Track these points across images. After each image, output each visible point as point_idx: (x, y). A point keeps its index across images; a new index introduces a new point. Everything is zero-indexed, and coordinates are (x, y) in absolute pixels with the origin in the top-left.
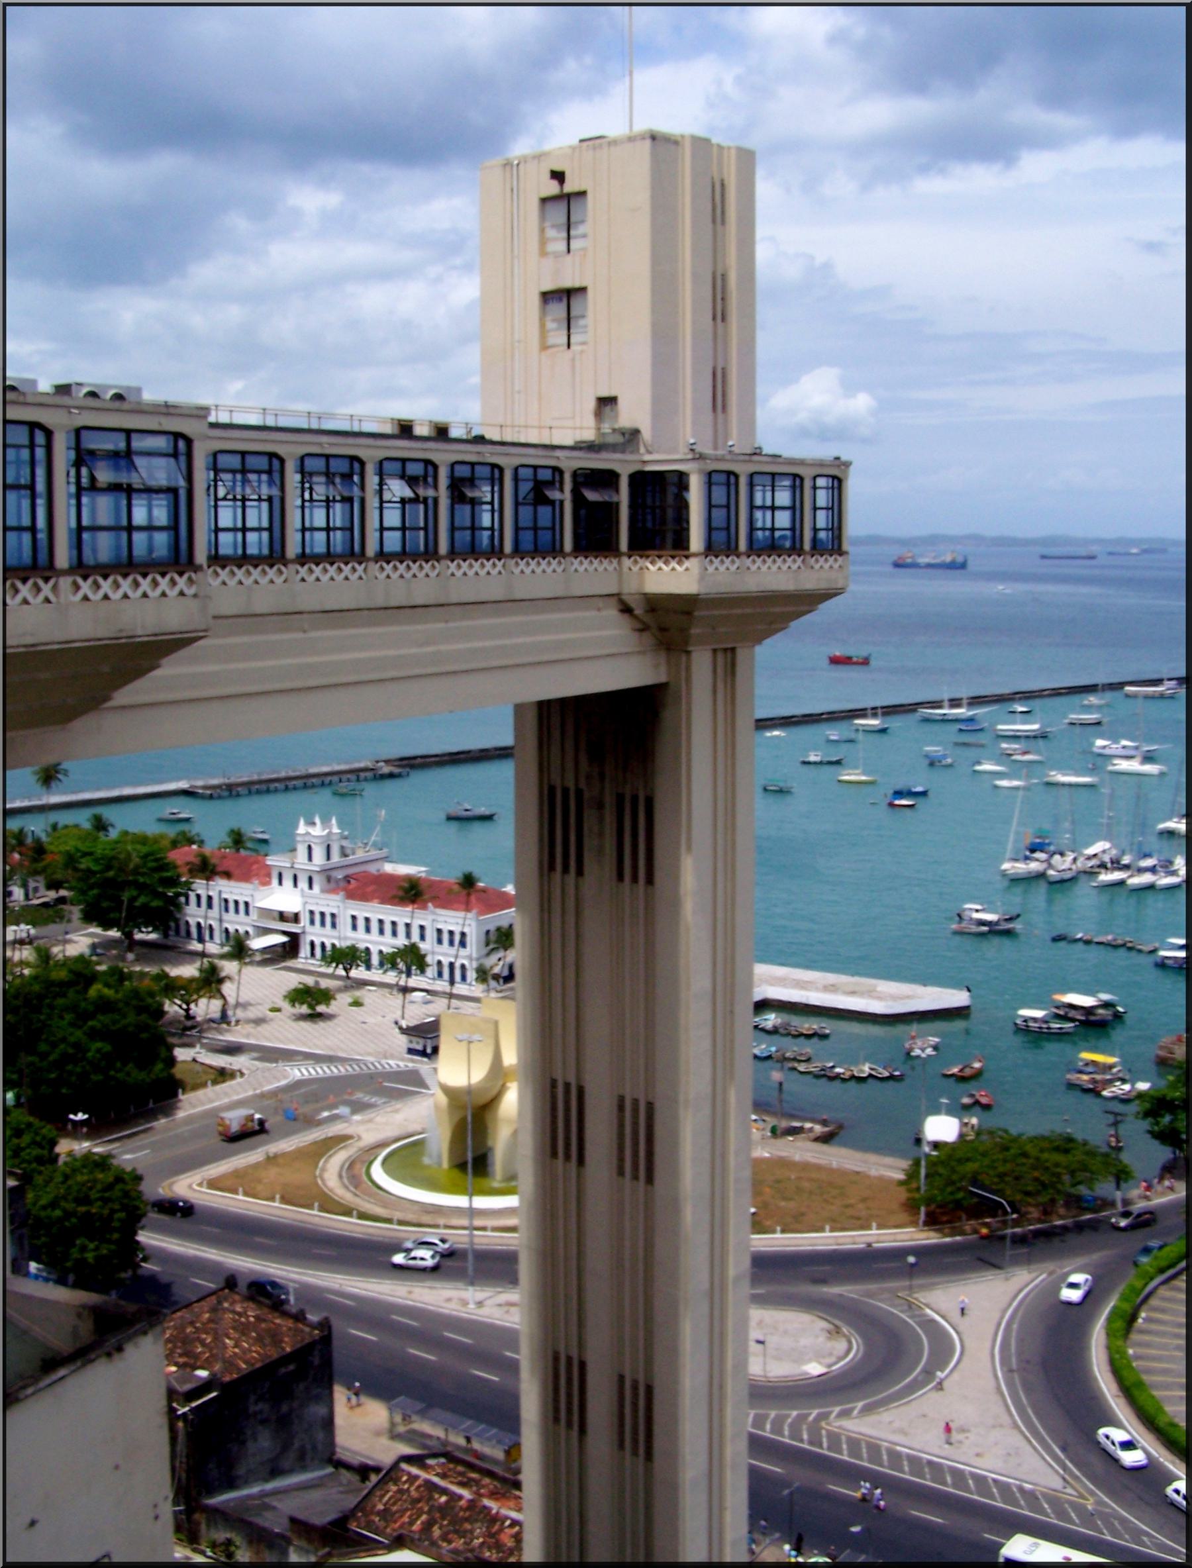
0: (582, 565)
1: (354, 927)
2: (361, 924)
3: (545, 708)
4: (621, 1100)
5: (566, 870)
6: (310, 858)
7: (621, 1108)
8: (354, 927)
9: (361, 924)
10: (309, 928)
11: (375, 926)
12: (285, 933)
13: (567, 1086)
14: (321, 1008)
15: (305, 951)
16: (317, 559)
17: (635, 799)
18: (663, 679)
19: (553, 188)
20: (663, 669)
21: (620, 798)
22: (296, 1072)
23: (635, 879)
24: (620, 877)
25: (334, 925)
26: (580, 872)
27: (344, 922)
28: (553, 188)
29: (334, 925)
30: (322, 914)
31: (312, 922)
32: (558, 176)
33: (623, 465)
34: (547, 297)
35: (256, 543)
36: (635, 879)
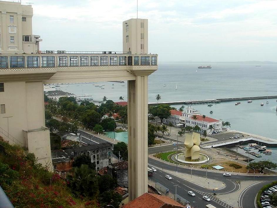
1: (192, 123)
6: (188, 112)
8: (192, 123)
12: (183, 124)
15: (185, 126)
18: (135, 79)
20: (135, 78)
22: (174, 143)
28: (126, 25)
30: (188, 121)
34: (127, 36)
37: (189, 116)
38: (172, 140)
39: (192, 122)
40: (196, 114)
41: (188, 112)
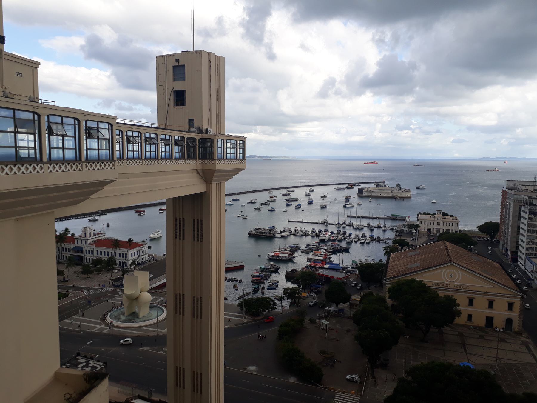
0: (187, 161)
1: (98, 254)
2: (99, 253)
3: (174, 199)
4: (194, 297)
5: (180, 239)
6: (85, 236)
7: (194, 300)
8: (98, 254)
9: (99, 253)
10: (85, 254)
11: (103, 253)
13: (180, 294)
14: (90, 275)
15: (84, 260)
16: (131, 159)
17: (198, 221)
19: (177, 64)
21: (194, 220)
23: (198, 241)
24: (194, 240)
25: (92, 254)
26: (183, 239)
27: (95, 253)
29: (92, 254)
31: (86, 253)
33: (197, 136)
35: (104, 153)
36: (198, 241)
37: (88, 242)
38: (80, 289)
39: (97, 251)
40: (103, 237)
41: (85, 236)
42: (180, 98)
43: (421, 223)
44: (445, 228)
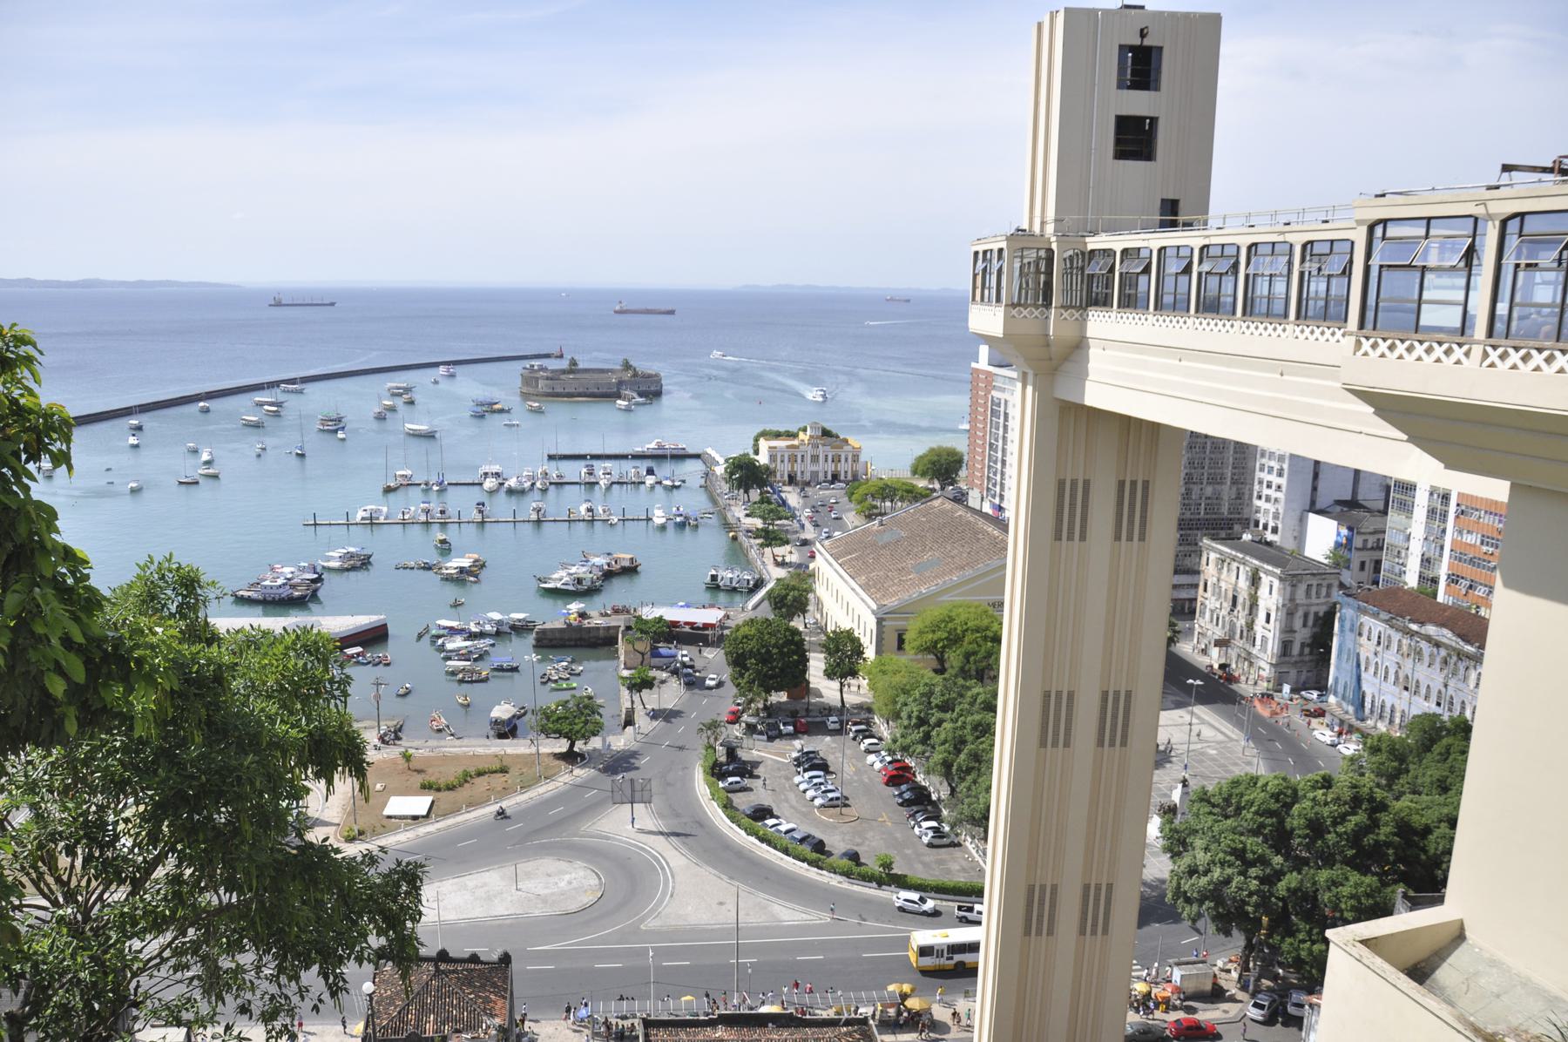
17: (1134, 483)
21: (1121, 484)
24: (1118, 538)
32: (1143, 34)
36: (1130, 538)
42: (1135, 139)
43: (773, 458)
44: (830, 467)
